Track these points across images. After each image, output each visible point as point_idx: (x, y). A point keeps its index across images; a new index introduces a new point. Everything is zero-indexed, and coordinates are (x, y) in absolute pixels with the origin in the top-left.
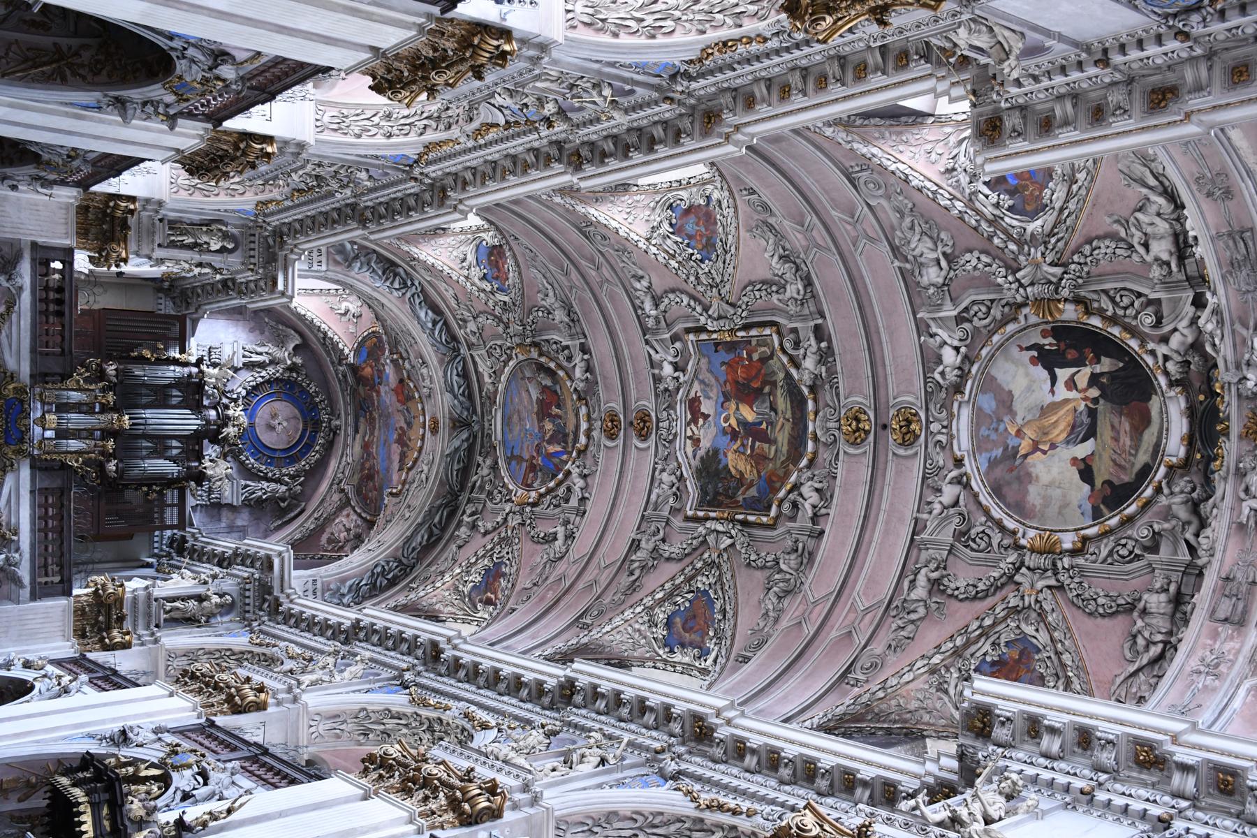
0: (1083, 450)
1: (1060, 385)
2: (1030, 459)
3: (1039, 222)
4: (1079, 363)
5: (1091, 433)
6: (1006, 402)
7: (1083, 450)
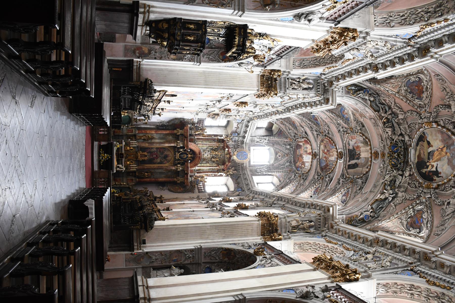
0: (431, 149)
1: (435, 166)
2: (443, 146)
3: (420, 207)
4: (430, 171)
5: (429, 153)
7: (431, 149)
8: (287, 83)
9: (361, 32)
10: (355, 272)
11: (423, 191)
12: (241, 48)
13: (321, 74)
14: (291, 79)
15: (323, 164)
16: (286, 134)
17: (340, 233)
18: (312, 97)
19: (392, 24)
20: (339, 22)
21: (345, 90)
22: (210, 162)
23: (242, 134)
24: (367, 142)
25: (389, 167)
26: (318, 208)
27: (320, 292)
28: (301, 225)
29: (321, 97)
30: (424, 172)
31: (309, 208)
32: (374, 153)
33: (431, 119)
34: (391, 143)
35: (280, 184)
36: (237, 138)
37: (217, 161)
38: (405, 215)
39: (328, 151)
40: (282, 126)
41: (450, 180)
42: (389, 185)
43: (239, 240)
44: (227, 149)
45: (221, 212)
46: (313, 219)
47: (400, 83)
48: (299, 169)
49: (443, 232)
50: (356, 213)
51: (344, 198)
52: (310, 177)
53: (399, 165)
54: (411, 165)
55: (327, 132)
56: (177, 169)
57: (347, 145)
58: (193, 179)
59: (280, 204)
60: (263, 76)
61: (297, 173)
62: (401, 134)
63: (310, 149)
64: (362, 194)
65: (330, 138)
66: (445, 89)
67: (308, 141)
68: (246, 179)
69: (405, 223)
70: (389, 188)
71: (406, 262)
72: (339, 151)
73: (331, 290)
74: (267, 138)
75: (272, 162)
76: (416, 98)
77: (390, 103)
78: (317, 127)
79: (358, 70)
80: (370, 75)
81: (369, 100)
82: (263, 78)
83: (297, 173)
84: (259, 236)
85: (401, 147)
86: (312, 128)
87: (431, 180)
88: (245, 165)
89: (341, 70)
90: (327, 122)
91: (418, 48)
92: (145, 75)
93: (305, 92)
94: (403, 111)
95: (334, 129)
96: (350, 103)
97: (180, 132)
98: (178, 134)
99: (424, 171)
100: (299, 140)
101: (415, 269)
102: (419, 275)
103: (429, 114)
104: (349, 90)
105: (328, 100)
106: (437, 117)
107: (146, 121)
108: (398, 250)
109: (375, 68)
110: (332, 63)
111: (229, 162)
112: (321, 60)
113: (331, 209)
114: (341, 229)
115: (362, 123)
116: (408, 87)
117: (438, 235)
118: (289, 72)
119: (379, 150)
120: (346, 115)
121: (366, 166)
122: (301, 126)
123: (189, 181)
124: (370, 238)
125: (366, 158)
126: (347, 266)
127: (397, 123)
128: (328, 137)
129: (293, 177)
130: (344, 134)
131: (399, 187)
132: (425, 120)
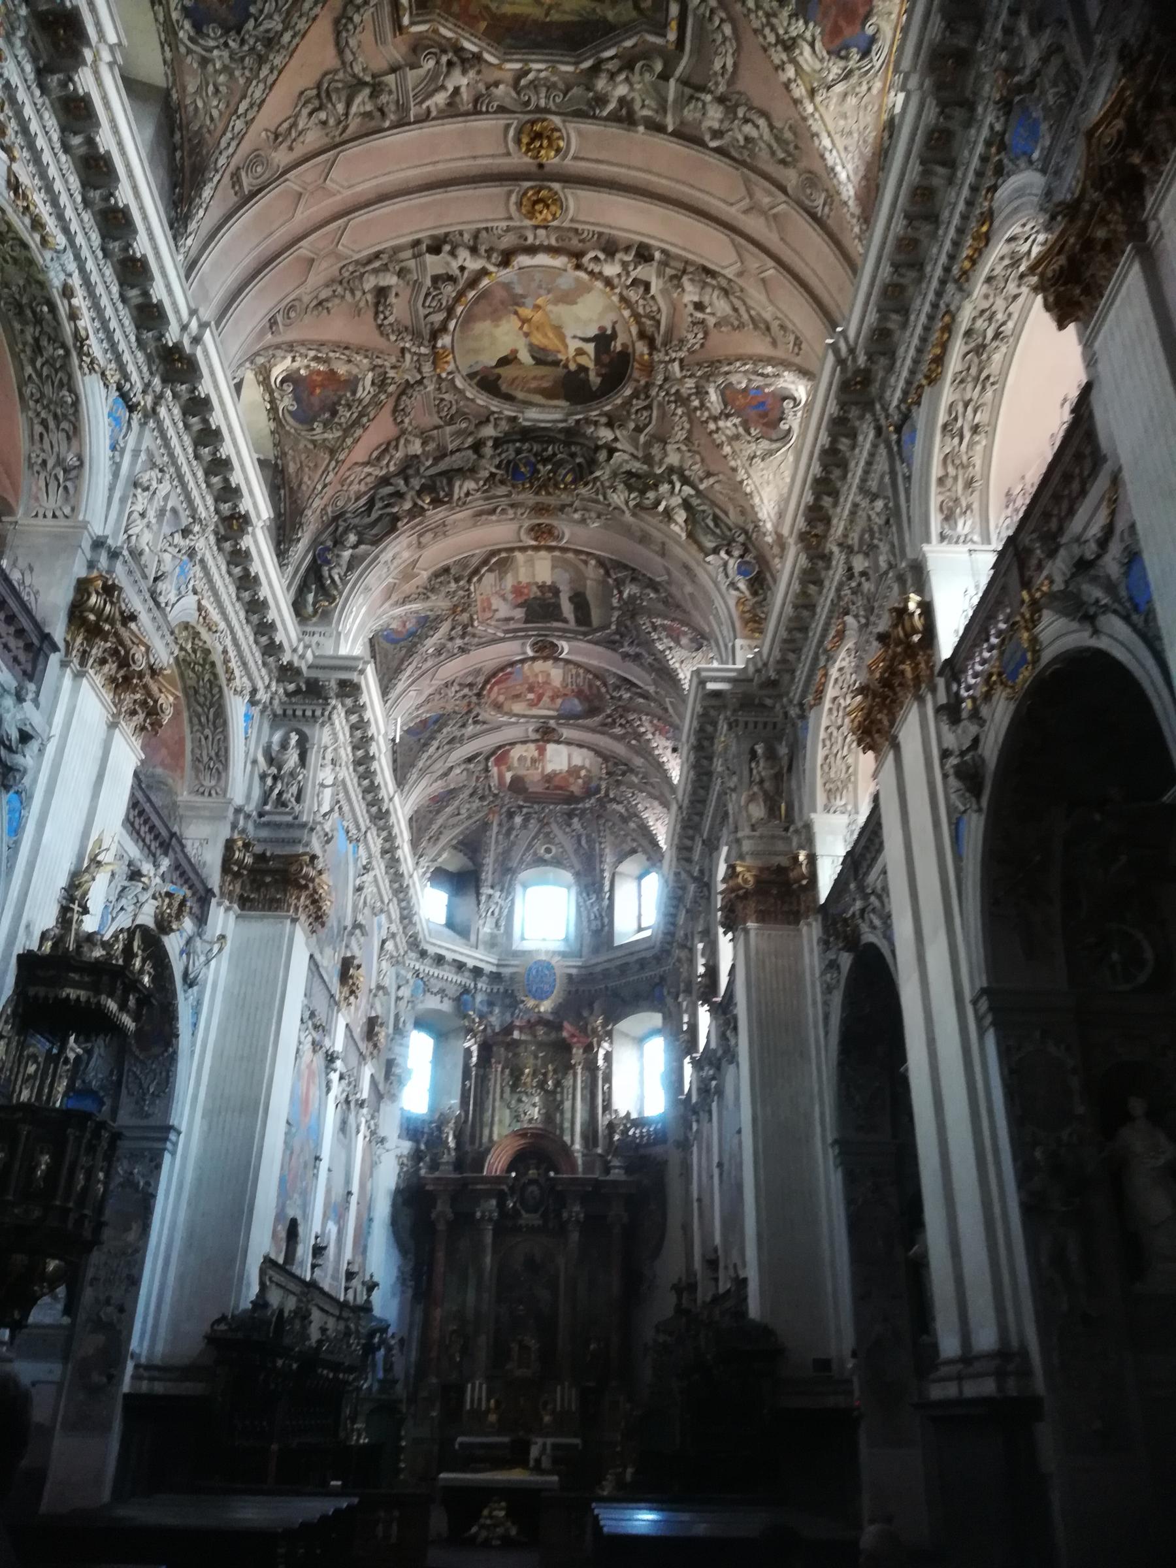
0: (525, 357)
1: (580, 344)
2: (514, 318)
4: (598, 361)
5: (539, 362)
6: (568, 298)
7: (525, 357)
8: (277, 818)
9: (91, 565)
10: (902, 613)
11: (661, 387)
12: (105, 979)
13: (253, 702)
14: (265, 803)
15: (577, 705)
16: (474, 827)
17: (791, 657)
18: (331, 737)
19: (71, 460)
20: (46, 637)
21: (315, 624)
22: (558, 1097)
23: (465, 979)
24: (498, 560)
25: (584, 491)
26: (710, 728)
27: (959, 731)
28: (767, 785)
29: (334, 708)
30: (599, 380)
31: (710, 758)
32: (536, 539)
33: (423, 350)
34: (502, 482)
35: (645, 852)
36: (479, 998)
37: (555, 1071)
38: (737, 445)
39: (531, 689)
40: (444, 840)
41: (623, 299)
42: (643, 493)
43: (814, 1003)
44: (516, 1035)
45: (724, 1062)
46: (746, 747)
47: (301, 446)
48: (593, 784)
49: (790, 326)
50: (732, 603)
51: (684, 641)
52: (620, 749)
53: (578, 460)
54: (578, 421)
55: (466, 691)
56: (578, 1221)
57: (512, 625)
58: (616, 1162)
59: (702, 854)
60: (244, 903)
61: (607, 795)
62: (477, 447)
63: (525, 747)
64: (669, 583)
65: (487, 682)
66: (320, 303)
67: (500, 754)
68: (623, 969)
69: (765, 445)
70: (651, 495)
71: (875, 446)
72: (530, 653)
73: (957, 693)
74: (486, 891)
75: (568, 876)
76: (354, 393)
77: (369, 479)
78: (451, 723)
79: (240, 578)
80: (259, 542)
81: (355, 547)
82: (252, 900)
83: (607, 795)
84: (799, 931)
85: (518, 452)
86: (453, 739)
87: (625, 357)
88: (574, 971)
89: (240, 634)
90: (431, 690)
91: (165, 381)
92: (192, 1347)
93: (312, 757)
94: (398, 439)
95: (455, 668)
96: (364, 610)
97: (442, 1208)
98: (451, 1216)
99: (594, 379)
100: (494, 782)
101: (896, 417)
102: (914, 408)
103: (408, 356)
104: (315, 612)
105: (343, 684)
106: (416, 335)
107: (393, 1342)
108: (837, 473)
109: (233, 524)
110: (213, 664)
111: (560, 1028)
112: (202, 699)
113: (711, 686)
114: (777, 654)
115: (436, 575)
116: (314, 420)
117: (798, 343)
118: (238, 811)
119: (527, 524)
120: (408, 625)
121: (582, 566)
122: (446, 774)
123: (623, 1178)
124: (803, 561)
125: (553, 567)
126: (883, 638)
127: (437, 460)
128: (483, 688)
129: (620, 808)
130: (474, 636)
131: (648, 459)
132: (427, 369)
